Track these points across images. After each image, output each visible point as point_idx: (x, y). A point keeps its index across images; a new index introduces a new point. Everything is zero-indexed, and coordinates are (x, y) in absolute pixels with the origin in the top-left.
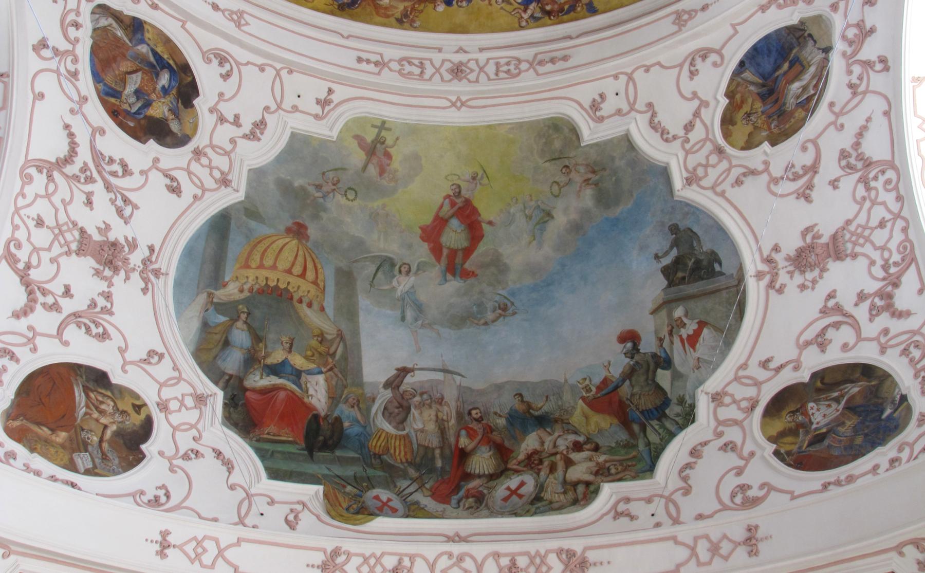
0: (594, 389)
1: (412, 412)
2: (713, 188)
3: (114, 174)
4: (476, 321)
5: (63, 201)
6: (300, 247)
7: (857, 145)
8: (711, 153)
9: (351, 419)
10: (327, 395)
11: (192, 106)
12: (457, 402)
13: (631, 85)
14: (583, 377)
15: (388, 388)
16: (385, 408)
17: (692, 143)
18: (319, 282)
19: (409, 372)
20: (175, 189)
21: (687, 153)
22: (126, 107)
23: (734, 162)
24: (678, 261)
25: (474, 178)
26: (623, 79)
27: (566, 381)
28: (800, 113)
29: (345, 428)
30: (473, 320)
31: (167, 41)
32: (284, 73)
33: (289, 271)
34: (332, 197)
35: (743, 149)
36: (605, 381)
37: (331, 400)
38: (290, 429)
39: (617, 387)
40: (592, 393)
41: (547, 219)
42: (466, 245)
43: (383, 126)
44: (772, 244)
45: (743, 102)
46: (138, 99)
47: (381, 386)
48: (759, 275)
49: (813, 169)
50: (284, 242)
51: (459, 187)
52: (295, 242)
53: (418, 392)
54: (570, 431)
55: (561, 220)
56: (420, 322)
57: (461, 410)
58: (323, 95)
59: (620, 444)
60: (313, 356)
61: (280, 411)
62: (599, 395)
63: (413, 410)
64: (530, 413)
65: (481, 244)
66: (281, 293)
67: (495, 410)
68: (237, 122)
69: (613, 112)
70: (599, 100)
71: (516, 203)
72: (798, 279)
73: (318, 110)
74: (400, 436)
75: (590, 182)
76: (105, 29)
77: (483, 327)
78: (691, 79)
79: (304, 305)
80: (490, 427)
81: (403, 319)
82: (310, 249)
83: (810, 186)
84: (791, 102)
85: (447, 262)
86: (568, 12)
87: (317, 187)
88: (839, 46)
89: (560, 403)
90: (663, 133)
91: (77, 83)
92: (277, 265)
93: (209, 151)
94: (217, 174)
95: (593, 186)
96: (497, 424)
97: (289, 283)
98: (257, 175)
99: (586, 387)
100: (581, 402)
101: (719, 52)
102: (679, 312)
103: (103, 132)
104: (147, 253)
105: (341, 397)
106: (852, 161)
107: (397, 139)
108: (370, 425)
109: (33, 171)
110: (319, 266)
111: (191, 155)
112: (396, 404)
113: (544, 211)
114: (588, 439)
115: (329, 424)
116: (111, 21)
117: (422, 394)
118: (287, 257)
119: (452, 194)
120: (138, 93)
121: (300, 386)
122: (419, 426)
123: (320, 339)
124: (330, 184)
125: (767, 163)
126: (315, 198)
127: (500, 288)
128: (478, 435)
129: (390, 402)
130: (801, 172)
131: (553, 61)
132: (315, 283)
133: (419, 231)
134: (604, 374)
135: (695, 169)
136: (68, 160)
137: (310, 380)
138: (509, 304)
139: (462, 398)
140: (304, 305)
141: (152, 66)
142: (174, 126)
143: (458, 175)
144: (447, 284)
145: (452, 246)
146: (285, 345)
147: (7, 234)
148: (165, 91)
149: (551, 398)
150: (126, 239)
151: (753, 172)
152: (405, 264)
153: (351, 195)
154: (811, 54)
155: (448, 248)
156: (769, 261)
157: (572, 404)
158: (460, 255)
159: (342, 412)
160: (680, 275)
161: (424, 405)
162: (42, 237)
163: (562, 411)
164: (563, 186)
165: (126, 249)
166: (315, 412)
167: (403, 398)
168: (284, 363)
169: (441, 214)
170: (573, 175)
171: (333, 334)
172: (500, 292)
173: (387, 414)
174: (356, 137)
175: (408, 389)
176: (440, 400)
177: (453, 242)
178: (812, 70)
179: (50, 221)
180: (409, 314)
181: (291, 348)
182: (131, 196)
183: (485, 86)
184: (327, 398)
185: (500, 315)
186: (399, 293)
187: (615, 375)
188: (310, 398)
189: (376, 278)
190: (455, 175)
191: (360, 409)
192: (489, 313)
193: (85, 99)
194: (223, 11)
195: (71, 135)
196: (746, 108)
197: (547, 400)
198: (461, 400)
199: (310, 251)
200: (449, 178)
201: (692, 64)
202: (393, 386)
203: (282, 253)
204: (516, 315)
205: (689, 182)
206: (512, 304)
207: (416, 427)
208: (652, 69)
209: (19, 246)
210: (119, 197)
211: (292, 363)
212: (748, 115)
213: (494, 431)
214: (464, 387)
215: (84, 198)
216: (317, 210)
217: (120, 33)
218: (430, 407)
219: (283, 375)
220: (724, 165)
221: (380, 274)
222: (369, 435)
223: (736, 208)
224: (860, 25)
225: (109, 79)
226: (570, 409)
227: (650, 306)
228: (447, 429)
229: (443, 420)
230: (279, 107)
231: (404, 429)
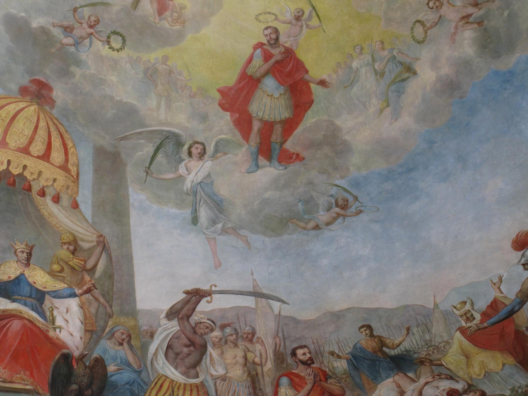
0: (478, 317)
1: (208, 353)
4: (302, 224)
6: (42, 116)
9: (119, 361)
10: (83, 327)
12: (274, 338)
14: (461, 300)
15: (172, 319)
16: (169, 347)
18: (70, 167)
19: (204, 296)
25: (298, 18)
27: (436, 305)
29: (109, 375)
30: (298, 222)
33: (25, 150)
34: (88, 44)
36: (494, 305)
37: (88, 335)
38: (28, 373)
39: (512, 313)
40: (475, 322)
41: (407, 75)
42: (287, 116)
47: (163, 315)
50: (18, 108)
51: (276, 31)
52: (33, 108)
53: (218, 324)
54: (443, 376)
56: (219, 226)
57: (282, 349)
59: (517, 391)
60: (62, 271)
61: (13, 348)
62: (485, 325)
63: (210, 349)
64: (384, 353)
65: (309, 113)
66: (14, 180)
67: (331, 349)
71: (361, 53)
74: (191, 385)
75: (471, 19)
77: (314, 232)
79: (48, 200)
80: (324, 372)
81: (195, 220)
82: (56, 119)
85: (258, 140)
87: (65, 30)
89: (427, 337)
92: (8, 140)
95: (476, 26)
96: (333, 368)
97: (25, 167)
99: (465, 314)
100: (458, 334)
105: (104, 330)
108: (147, 371)
110: (70, 144)
112: (185, 341)
113: (401, 63)
114: (470, 386)
115: (86, 367)
117: (223, 327)
119: (266, 42)
121: (42, 314)
122: (221, 371)
123: (71, 248)
124: (85, 25)
126: (63, 45)
127: (338, 176)
128: (306, 384)
129: (176, 337)
132: (64, 167)
133: (218, 96)
134: (493, 294)
137: (57, 305)
138: (351, 199)
139: (283, 332)
140: (48, 200)
143: (274, 14)
144: (259, 172)
145: (266, 117)
146: (20, 255)
149: (415, 330)
152: (198, 143)
153: (116, 43)
155: (261, 120)
157: (446, 339)
158: (278, 130)
159: (105, 351)
161: (226, 342)
163: (431, 348)
164: (431, 27)
166: (65, 351)
167: (195, 332)
168: (19, 280)
169: (250, 71)
170: (445, 10)
171: (92, 241)
172: (338, 182)
173: (171, 354)
175: (203, 321)
176: (250, 336)
177: (267, 112)
180: (204, 214)
181: (28, 259)
184: (83, 331)
185: (339, 215)
186: (188, 184)
187: (508, 296)
188: (58, 330)
189: (155, 162)
190: (269, 13)
191: (131, 347)
192: (321, 213)
197: (408, 334)
198: (280, 335)
199: (55, 121)
200: (262, 18)
202: (180, 316)
203: (15, 123)
204: (361, 215)
206: (356, 199)
207: (214, 373)
211: (30, 280)
213: (330, 377)
214: (286, 317)
218: (236, 345)
219: (16, 297)
221: (160, 157)
222: (145, 383)
226: (442, 345)
228: (260, 376)
229: (254, 363)
231: (197, 376)
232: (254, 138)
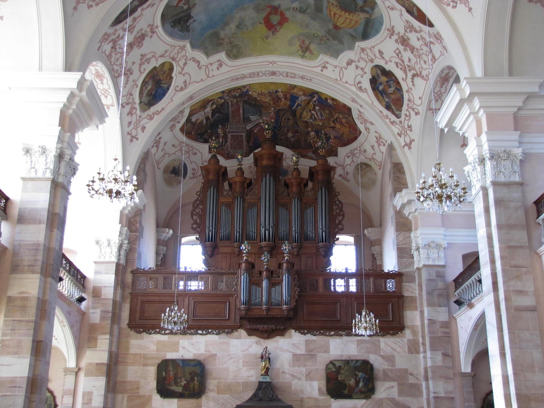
2: (175, 47)
3: (400, 64)
5: (417, 64)
7: (128, 77)
8: (177, 57)
11: (372, 76)
13: (208, 74)
17: (184, 59)
20: (381, 52)
21: (185, 55)
22: (394, 84)
23: (168, 57)
24: (187, 21)
26: (211, 76)
28: (147, 80)
31: (378, 99)
32: (339, 79)
35: (165, 62)
43: (302, 57)
44: (153, 38)
45: (167, 77)
46: (390, 85)
48: (157, 27)
49: (141, 65)
51: (273, 35)
52: (338, 24)
55: (233, 26)
58: (325, 70)
68: (357, 67)
69: (214, 64)
70: (219, 68)
72: (143, 32)
73: (327, 65)
76: (398, 111)
78: (186, 80)
79: (335, 5)
83: (141, 59)
84: (150, 82)
86: (231, 91)
88: (137, 106)
90: (194, 60)
91: (408, 97)
93: (367, 60)
94: (365, 52)
98: (351, 48)
101: (176, 91)
102: (186, 7)
103: (403, 79)
104: (392, 37)
106: (129, 73)
107: (297, 52)
109: (425, 77)
110: (329, 15)
111: (374, 61)
116: (396, 112)
118: (341, 20)
120: (390, 87)
125: (157, 60)
130: (145, 62)
131: (237, 79)
135: (182, 51)
136: (414, 76)
141: (385, 94)
142: (379, 72)
147: (434, 65)
148: (381, 84)
150: (398, 44)
151: (161, 56)
153: (316, 35)
154: (145, 99)
156: (153, 32)
160: (186, 18)
162: (425, 58)
165: (399, 41)
174: (313, 54)
178: (144, 95)
179: (422, 62)
182: (395, 55)
183: (263, 70)
193: (407, 91)
194: (358, 104)
195: (413, 82)
196: (165, 75)
201: (186, 85)
205: (184, 46)
208: (200, 80)
209: (432, 60)
210: (400, 57)
212: (164, 73)
215: (411, 62)
216: (329, 32)
217: (393, 107)
220: (171, 56)
223: (167, 44)
224: (132, 114)
225: (399, 95)
227: (197, 6)
230: (341, 69)
232: (280, 10)
